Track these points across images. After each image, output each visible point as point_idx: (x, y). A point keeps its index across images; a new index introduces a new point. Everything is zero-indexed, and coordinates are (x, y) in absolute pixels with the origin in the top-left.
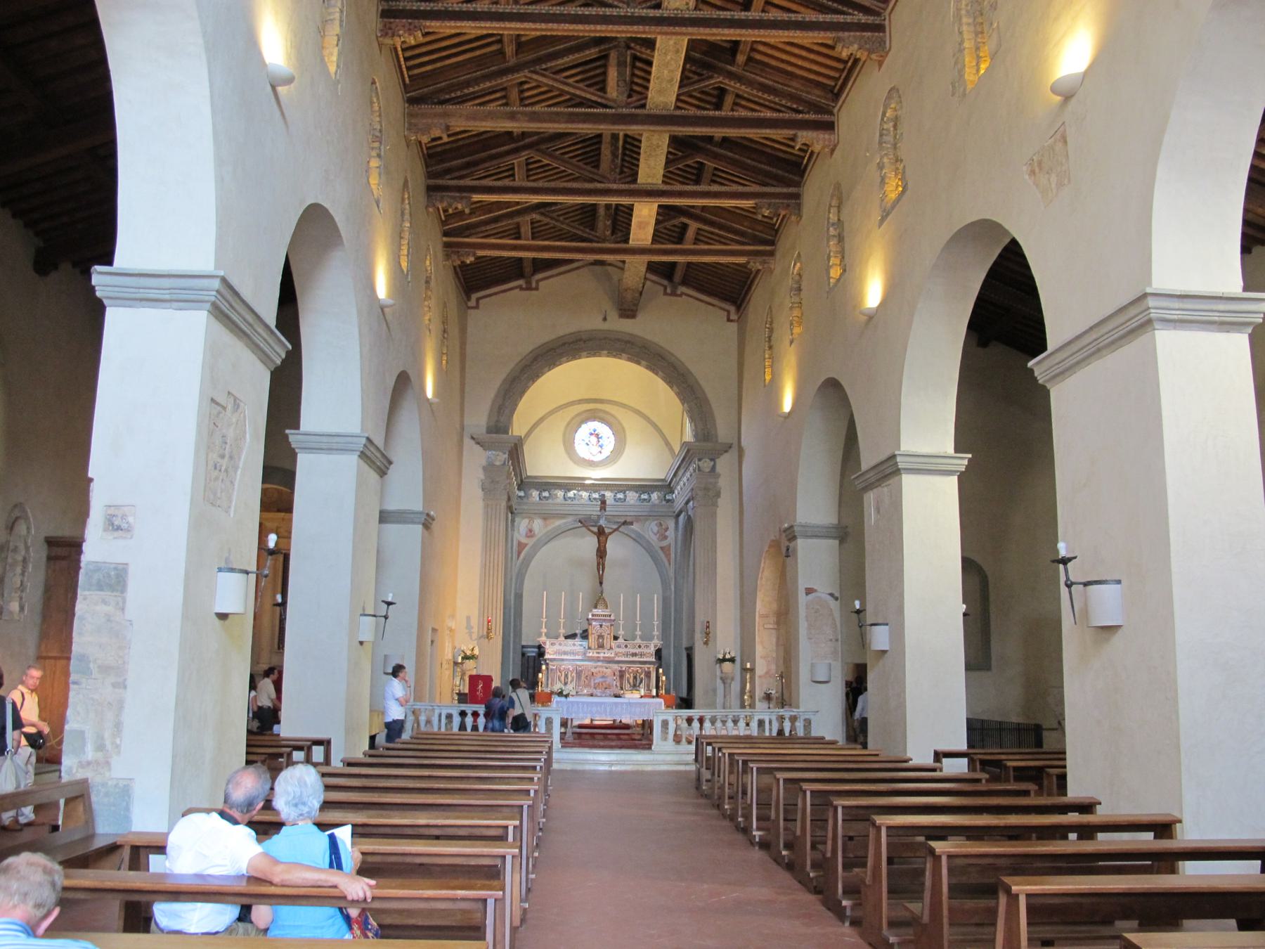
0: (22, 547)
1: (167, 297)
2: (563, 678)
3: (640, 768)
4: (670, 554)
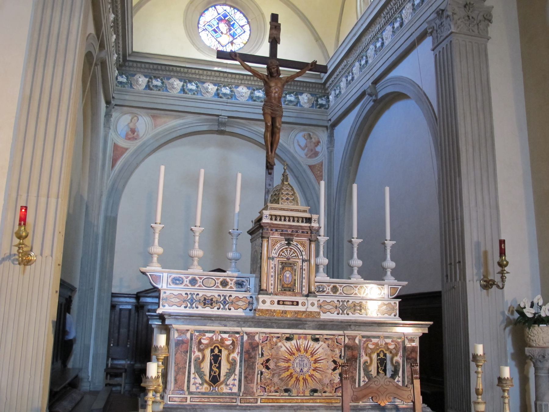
2: (206, 367)
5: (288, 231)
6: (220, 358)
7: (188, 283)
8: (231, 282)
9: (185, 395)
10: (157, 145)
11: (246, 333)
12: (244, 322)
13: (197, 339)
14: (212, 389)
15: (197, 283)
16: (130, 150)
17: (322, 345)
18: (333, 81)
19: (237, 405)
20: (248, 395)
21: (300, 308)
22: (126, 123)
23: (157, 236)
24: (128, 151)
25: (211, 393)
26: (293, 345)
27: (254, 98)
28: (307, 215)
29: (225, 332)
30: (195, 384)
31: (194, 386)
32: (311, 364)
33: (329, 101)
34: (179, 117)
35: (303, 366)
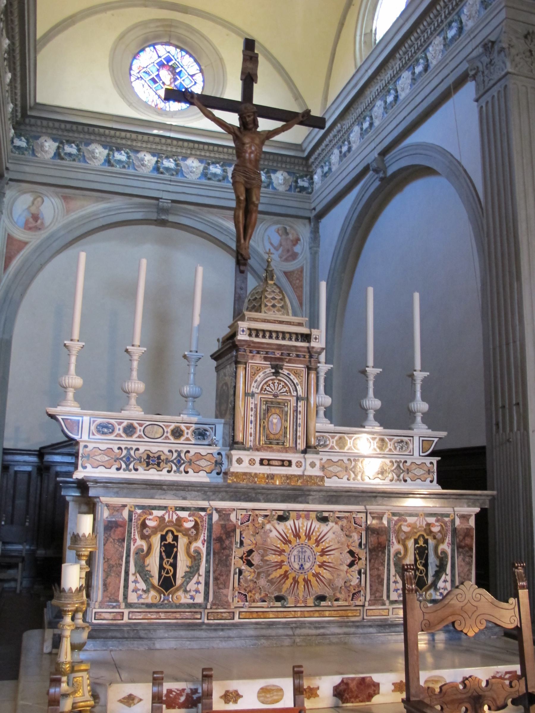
4: (302, 287)
5: (276, 354)
6: (175, 549)
7: (121, 432)
8: (188, 431)
9: (119, 608)
10: (70, 238)
11: (216, 509)
12: (214, 493)
13: (140, 519)
14: (162, 599)
15: (135, 433)
16: (31, 244)
17: (333, 527)
18: (319, 154)
19: (203, 623)
20: (219, 607)
21: (293, 470)
22: (25, 207)
23: (73, 359)
24: (27, 247)
25: (161, 605)
26: (289, 527)
27: (209, 176)
28: (304, 330)
29: (183, 509)
30: (135, 590)
31: (135, 594)
32: (316, 557)
33: (313, 182)
34: (103, 199)
35: (303, 560)
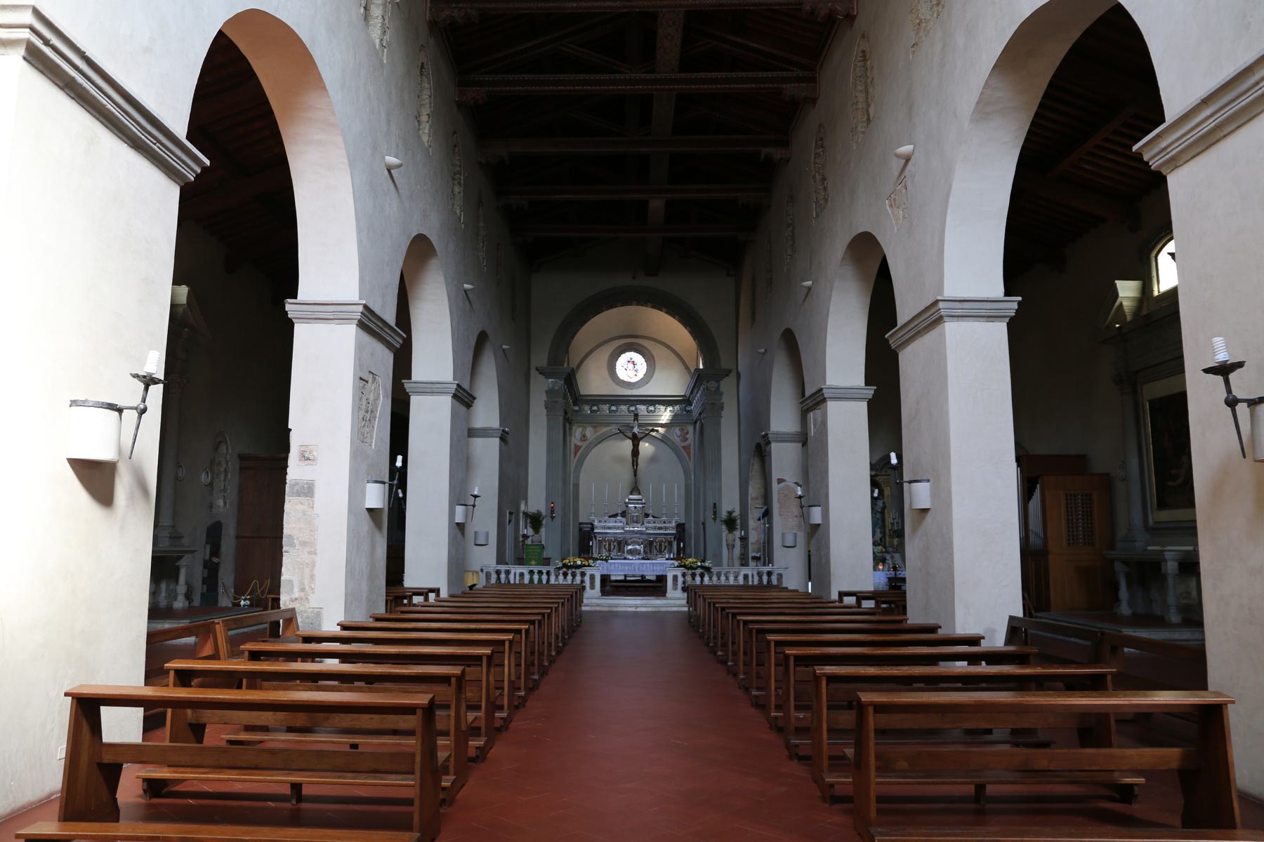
0: (224, 462)
1: (332, 317)
2: (607, 546)
3: (657, 609)
